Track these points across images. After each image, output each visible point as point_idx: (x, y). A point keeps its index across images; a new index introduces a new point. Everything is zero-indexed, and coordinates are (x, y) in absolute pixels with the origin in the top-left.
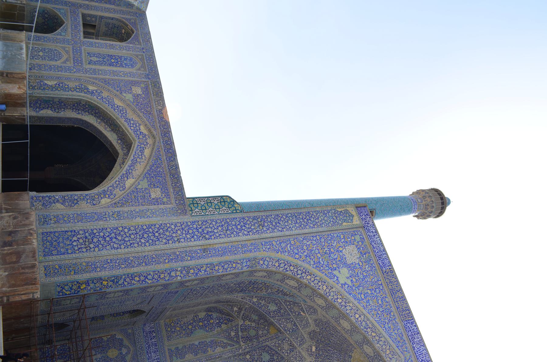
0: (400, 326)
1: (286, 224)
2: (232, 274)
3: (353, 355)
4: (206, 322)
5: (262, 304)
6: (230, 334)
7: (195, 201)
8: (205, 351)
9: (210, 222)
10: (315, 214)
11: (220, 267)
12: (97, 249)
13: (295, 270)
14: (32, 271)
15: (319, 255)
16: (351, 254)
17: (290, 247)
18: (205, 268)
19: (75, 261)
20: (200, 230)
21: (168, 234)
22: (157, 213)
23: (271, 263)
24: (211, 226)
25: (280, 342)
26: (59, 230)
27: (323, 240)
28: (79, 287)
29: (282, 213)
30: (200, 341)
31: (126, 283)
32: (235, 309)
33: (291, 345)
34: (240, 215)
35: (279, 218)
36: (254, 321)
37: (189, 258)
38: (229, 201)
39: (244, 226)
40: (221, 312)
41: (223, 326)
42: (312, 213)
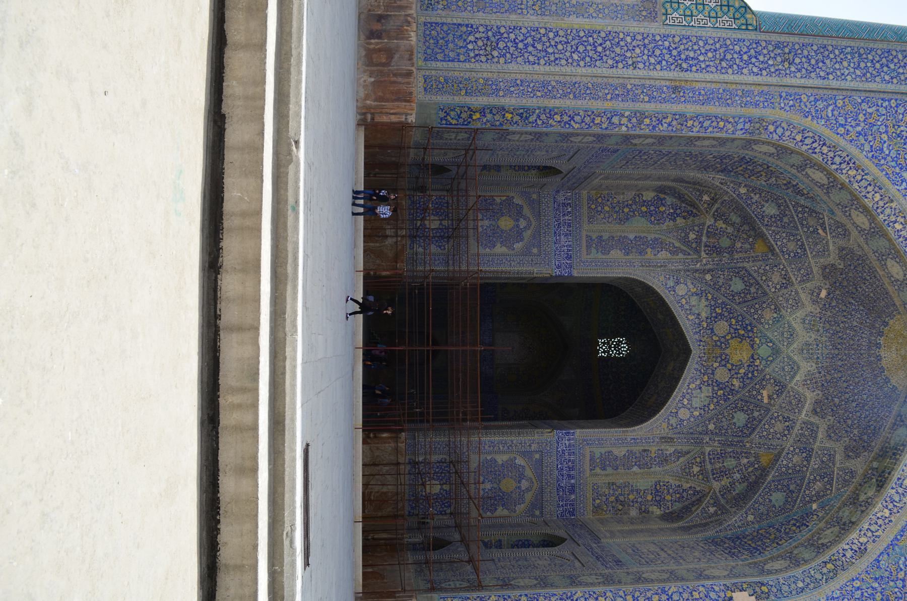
1: (837, 66)
2: (714, 138)
3: (891, 322)
4: (652, 208)
5: (754, 201)
6: (687, 235)
8: (642, 253)
10: (900, 57)
11: (696, 124)
12: (502, 60)
13: (831, 154)
14: (406, 80)
17: (832, 111)
18: (669, 119)
19: (467, 75)
20: (675, 53)
21: (618, 50)
22: (606, 11)
23: (787, 133)
24: (696, 47)
25: (767, 268)
26: (449, 20)
28: (471, 116)
29: (834, 43)
30: (638, 235)
31: (540, 122)
32: (706, 198)
33: (786, 277)
34: (752, 36)
35: (827, 53)
36: (733, 225)
37: (646, 99)
39: (756, 57)
40: (680, 197)
41: (679, 220)
42: (894, 53)
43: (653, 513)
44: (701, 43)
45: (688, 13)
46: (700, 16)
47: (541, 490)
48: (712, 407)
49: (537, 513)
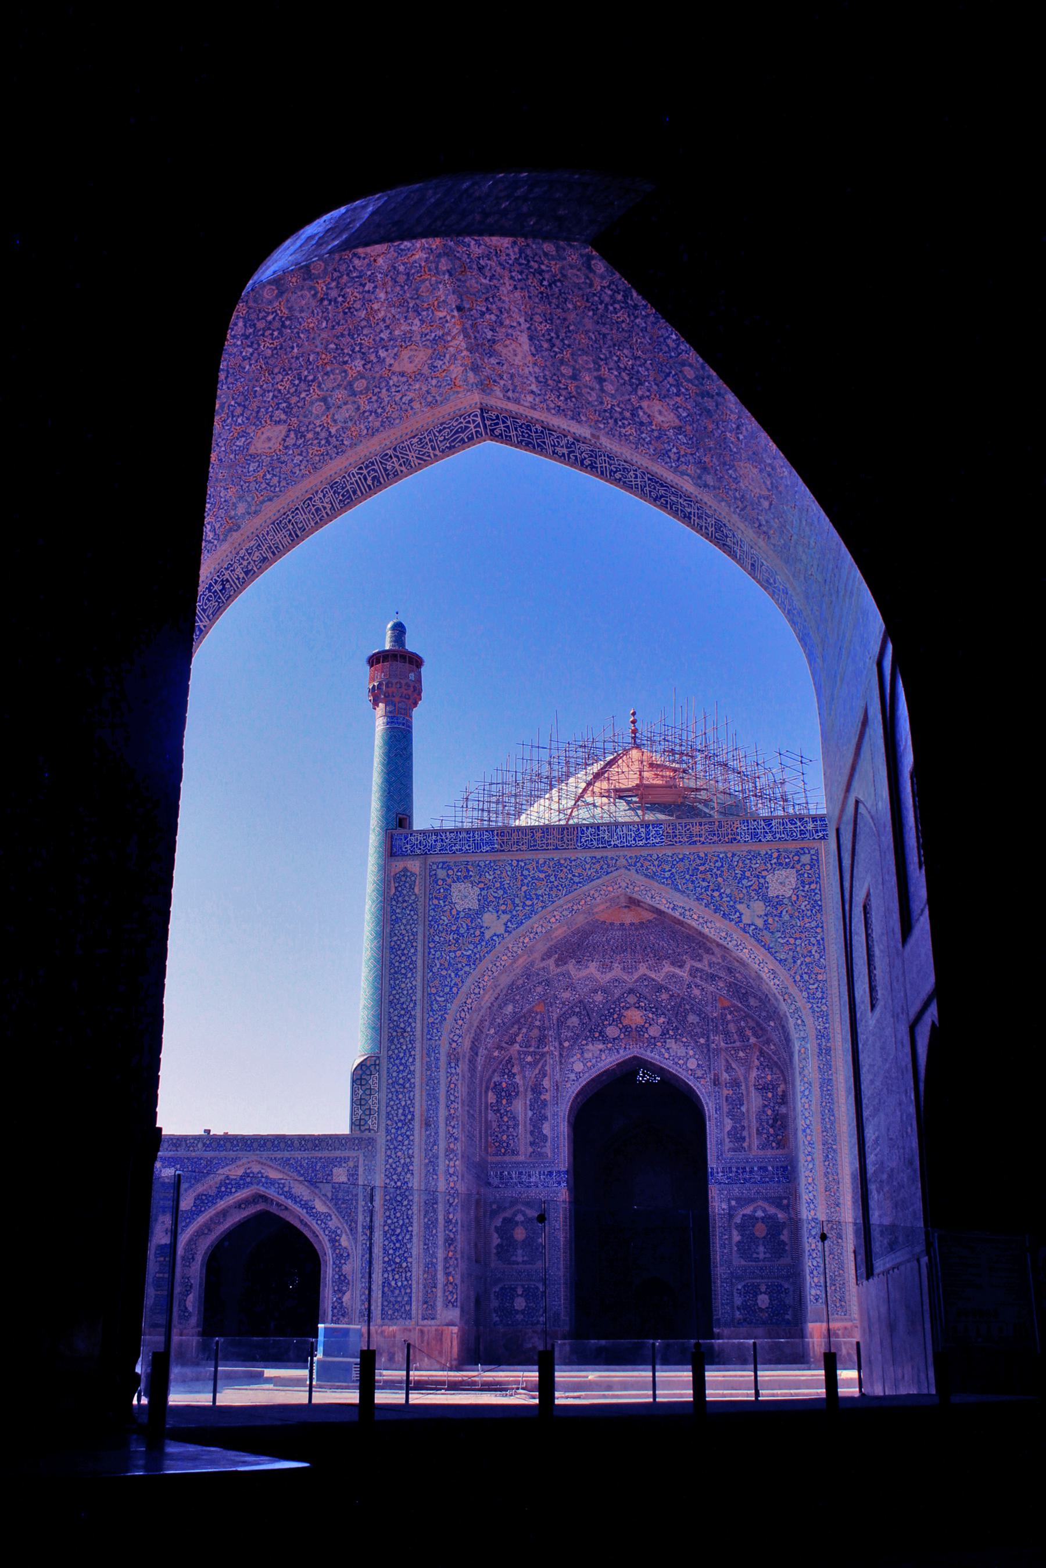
0: (583, 855)
4: (503, 1094)
6: (530, 1063)
7: (356, 1123)
8: (544, 1103)
9: (389, 1109)
10: (395, 938)
12: (409, 1260)
15: (458, 953)
16: (465, 896)
18: (450, 1128)
19: (421, 1286)
20: (400, 1124)
23: (458, 1031)
26: (380, 1300)
27: (437, 938)
36: (519, 1029)
38: (360, 1072)
41: (515, 1070)
42: (393, 944)
43: (783, 1091)
44: (392, 1103)
45: (367, 1112)
46: (370, 1102)
47: (766, 1199)
48: (684, 1040)
49: (785, 1202)
